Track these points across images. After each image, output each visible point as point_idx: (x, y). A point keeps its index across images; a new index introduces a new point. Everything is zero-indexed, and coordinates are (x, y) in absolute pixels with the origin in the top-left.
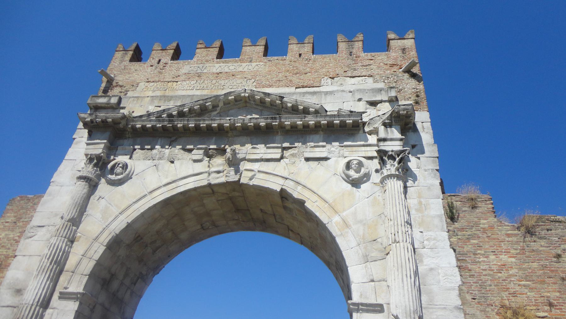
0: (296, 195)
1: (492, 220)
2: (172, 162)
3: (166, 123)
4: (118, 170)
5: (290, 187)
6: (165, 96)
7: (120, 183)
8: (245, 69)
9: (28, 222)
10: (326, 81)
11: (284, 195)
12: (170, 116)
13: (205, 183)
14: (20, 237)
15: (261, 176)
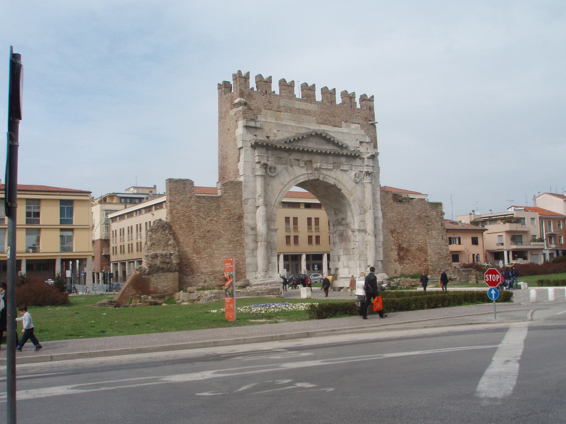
0: (339, 187)
1: (392, 201)
2: (292, 166)
3: (290, 146)
4: (272, 170)
5: (337, 182)
6: (278, 123)
7: (274, 177)
8: (310, 109)
9: (241, 196)
10: (343, 124)
11: (334, 186)
12: (290, 141)
13: (307, 179)
14: (241, 204)
15: (327, 177)
